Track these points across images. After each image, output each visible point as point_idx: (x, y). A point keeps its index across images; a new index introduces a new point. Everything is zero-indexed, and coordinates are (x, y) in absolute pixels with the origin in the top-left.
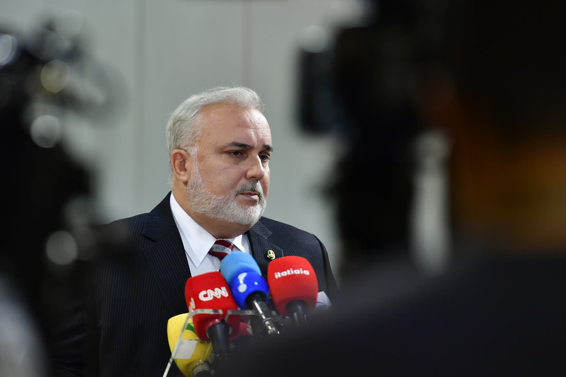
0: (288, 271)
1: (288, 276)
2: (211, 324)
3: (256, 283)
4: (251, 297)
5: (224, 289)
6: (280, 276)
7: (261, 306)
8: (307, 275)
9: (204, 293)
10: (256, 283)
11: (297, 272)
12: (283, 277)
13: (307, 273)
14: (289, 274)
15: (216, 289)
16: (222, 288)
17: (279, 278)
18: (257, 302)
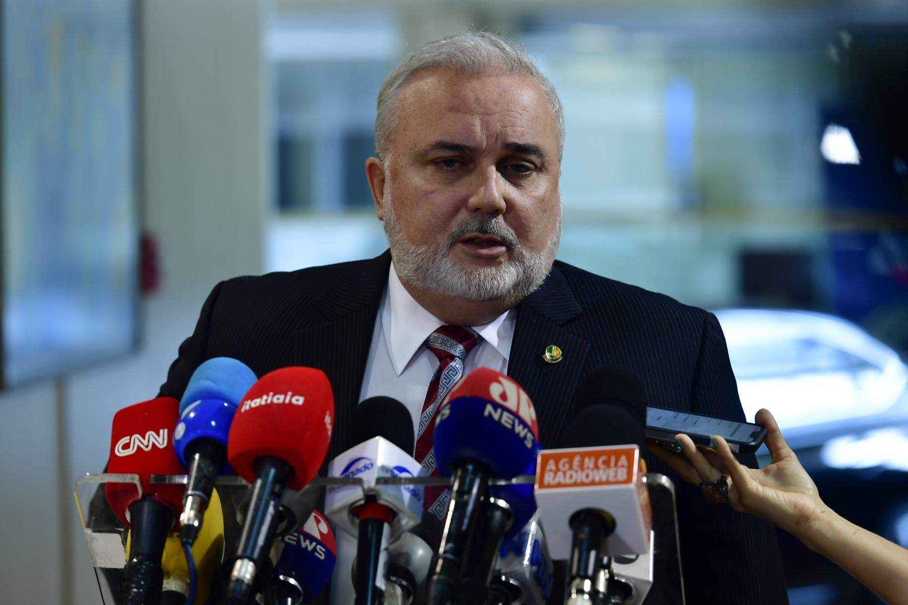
0: (265, 397)
1: (261, 407)
2: (131, 501)
3: (213, 423)
4: (192, 446)
5: (164, 432)
6: (247, 408)
7: (199, 467)
8: (298, 406)
9: (125, 440)
10: (213, 423)
11: (279, 399)
12: (251, 408)
13: (299, 400)
14: (263, 403)
15: (151, 434)
16: (161, 431)
17: (246, 411)
18: (200, 457)
